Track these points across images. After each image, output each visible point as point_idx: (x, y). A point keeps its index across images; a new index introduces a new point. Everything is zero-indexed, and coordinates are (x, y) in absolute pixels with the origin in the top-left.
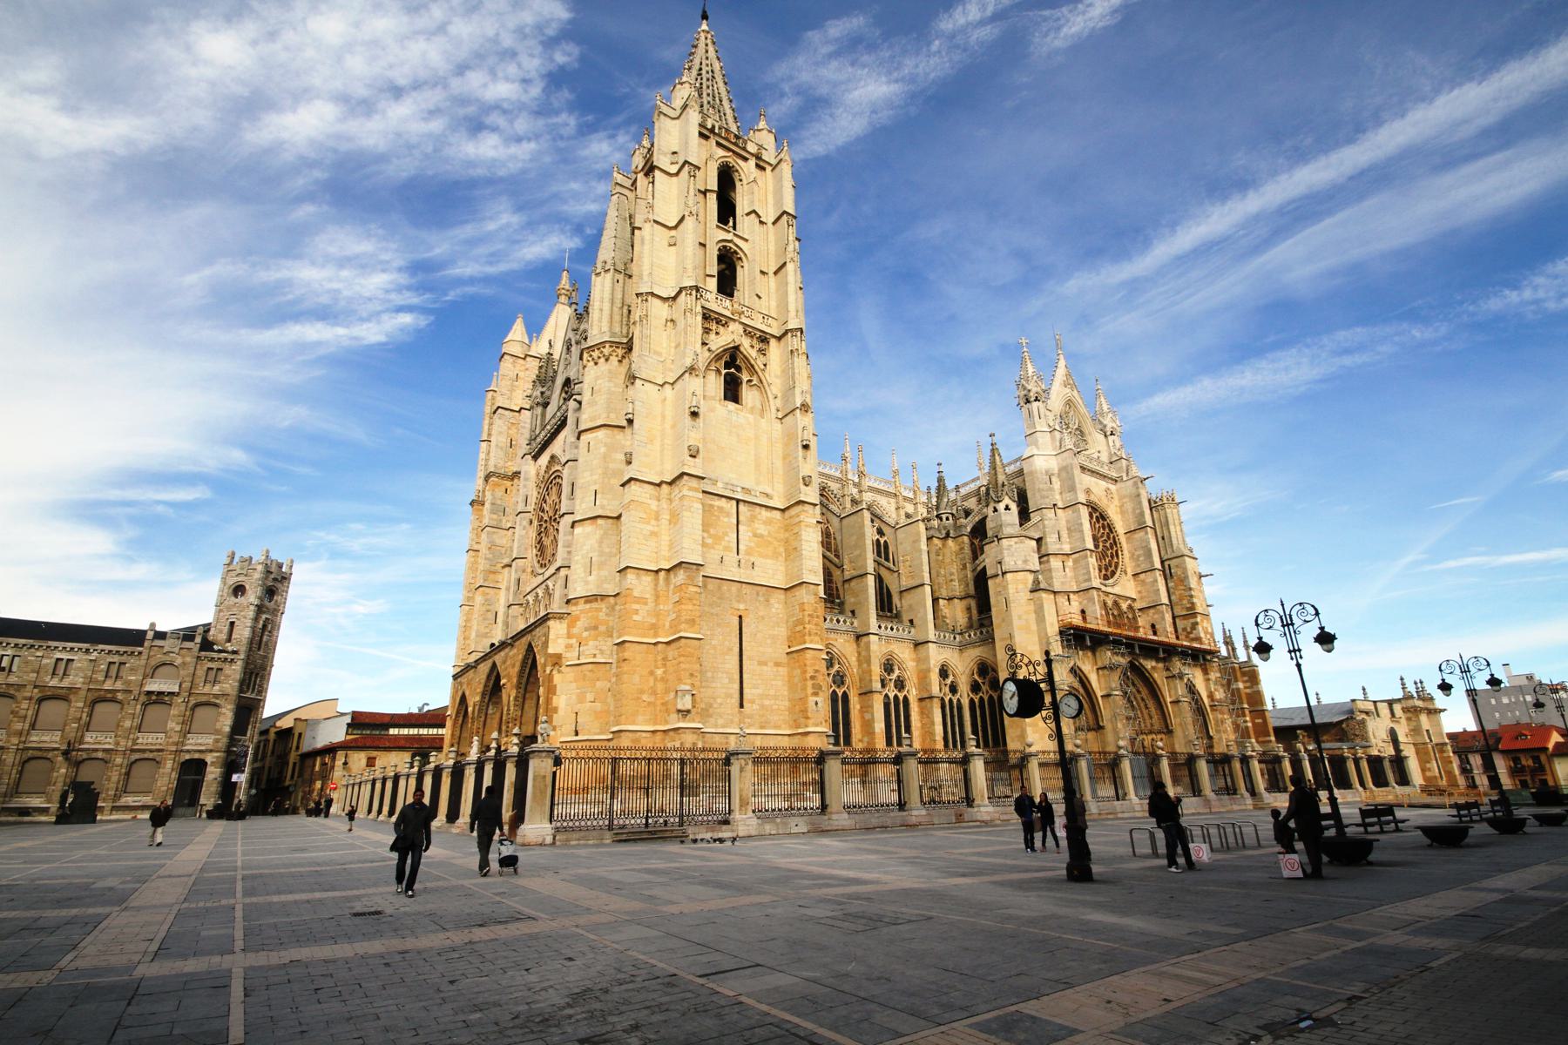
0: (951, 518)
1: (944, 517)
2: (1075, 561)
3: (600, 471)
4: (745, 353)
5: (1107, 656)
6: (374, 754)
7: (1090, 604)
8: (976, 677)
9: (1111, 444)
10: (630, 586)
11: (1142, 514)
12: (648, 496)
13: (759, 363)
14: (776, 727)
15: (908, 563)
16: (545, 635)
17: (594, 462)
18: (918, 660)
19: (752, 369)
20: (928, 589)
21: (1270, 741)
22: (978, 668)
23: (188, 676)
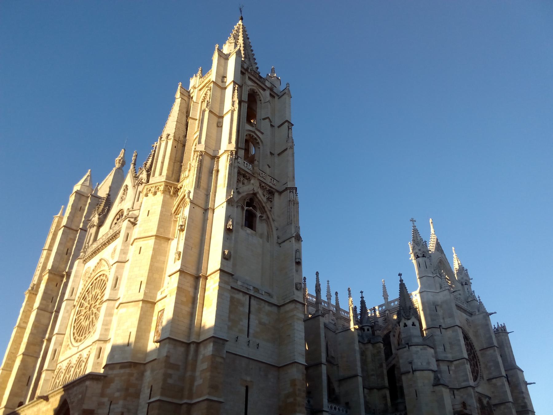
0: (370, 330)
1: (366, 328)
2: (456, 367)
3: (147, 267)
4: (260, 198)
13: (267, 206)
20: (360, 379)
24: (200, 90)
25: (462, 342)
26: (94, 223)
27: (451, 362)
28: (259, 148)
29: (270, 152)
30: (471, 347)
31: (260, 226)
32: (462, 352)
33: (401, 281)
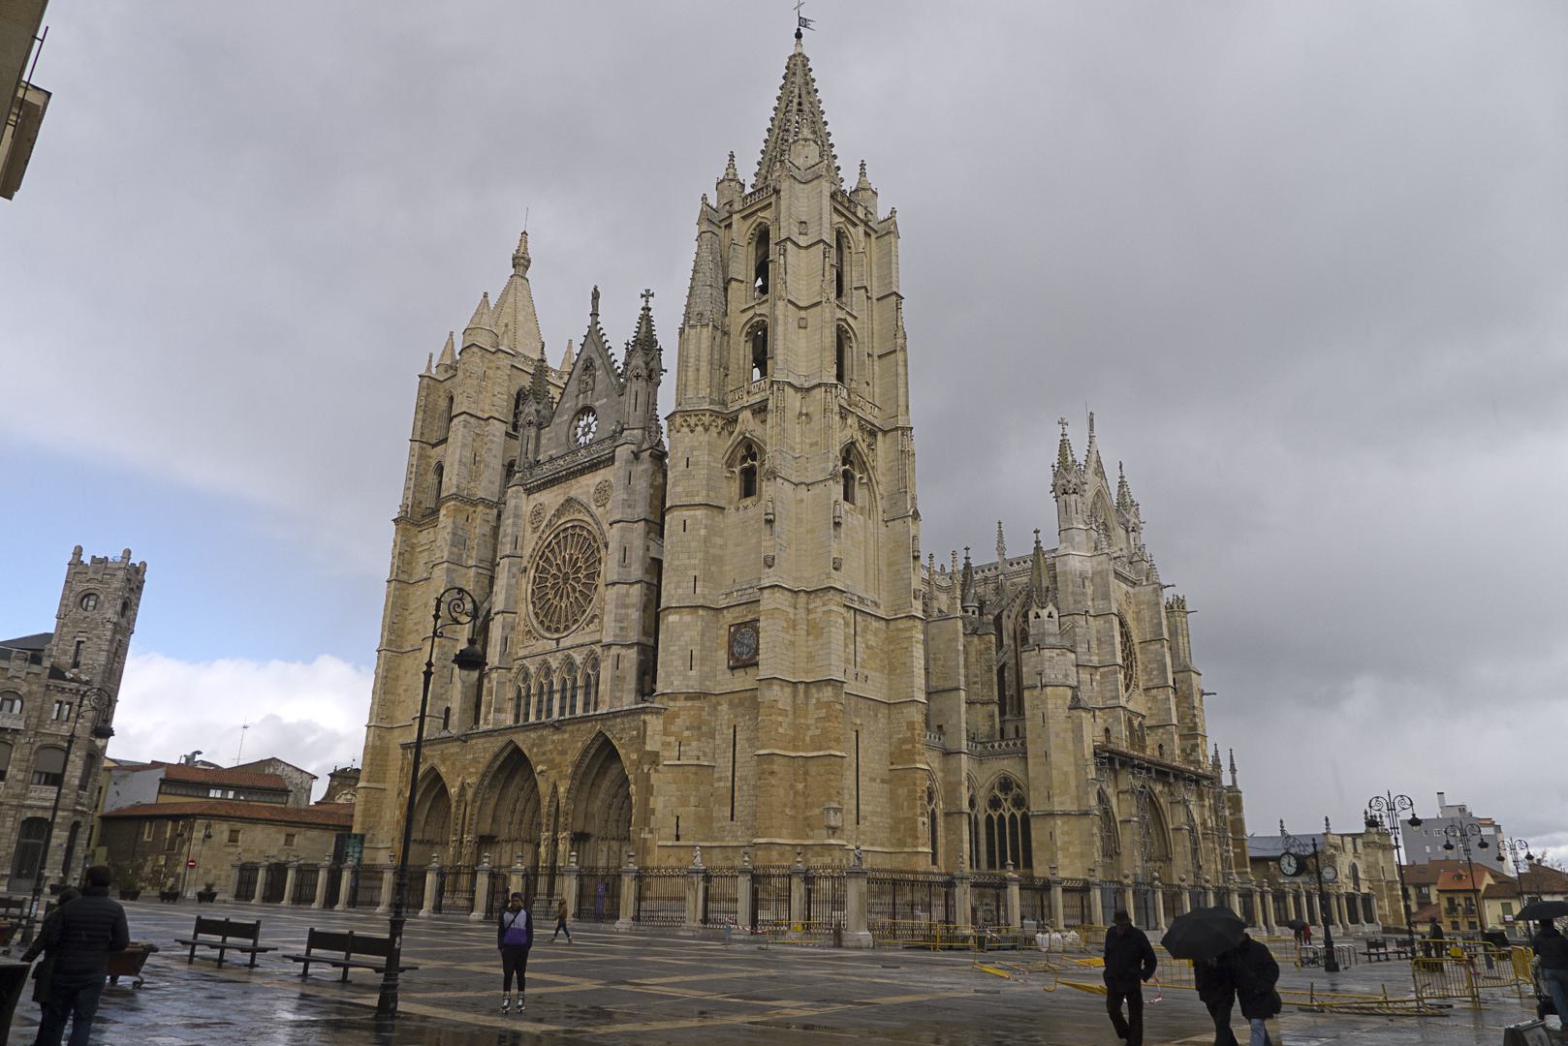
0: (977, 613)
1: (970, 610)
2: (1103, 675)
3: (700, 555)
5: (1127, 780)
6: (238, 825)
7: (1116, 723)
8: (997, 792)
9: (1132, 539)
10: (776, 698)
11: (1160, 624)
12: (787, 603)
13: (869, 459)
14: (881, 845)
15: (940, 663)
16: (637, 729)
17: (693, 544)
18: (946, 771)
19: (863, 468)
20: (963, 693)
21: (1247, 873)
22: (1000, 783)
23: (33, 710)
24: (744, 218)
25: (1118, 639)
26: (531, 418)
27: (1096, 668)
28: (851, 347)
29: (868, 354)
30: (1127, 638)
31: (860, 493)
32: (1115, 654)
33: (1036, 542)
